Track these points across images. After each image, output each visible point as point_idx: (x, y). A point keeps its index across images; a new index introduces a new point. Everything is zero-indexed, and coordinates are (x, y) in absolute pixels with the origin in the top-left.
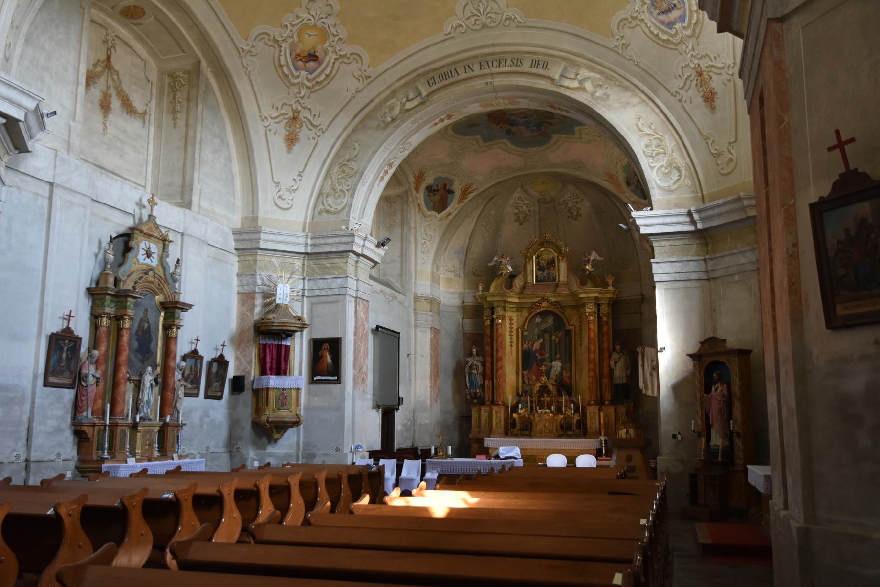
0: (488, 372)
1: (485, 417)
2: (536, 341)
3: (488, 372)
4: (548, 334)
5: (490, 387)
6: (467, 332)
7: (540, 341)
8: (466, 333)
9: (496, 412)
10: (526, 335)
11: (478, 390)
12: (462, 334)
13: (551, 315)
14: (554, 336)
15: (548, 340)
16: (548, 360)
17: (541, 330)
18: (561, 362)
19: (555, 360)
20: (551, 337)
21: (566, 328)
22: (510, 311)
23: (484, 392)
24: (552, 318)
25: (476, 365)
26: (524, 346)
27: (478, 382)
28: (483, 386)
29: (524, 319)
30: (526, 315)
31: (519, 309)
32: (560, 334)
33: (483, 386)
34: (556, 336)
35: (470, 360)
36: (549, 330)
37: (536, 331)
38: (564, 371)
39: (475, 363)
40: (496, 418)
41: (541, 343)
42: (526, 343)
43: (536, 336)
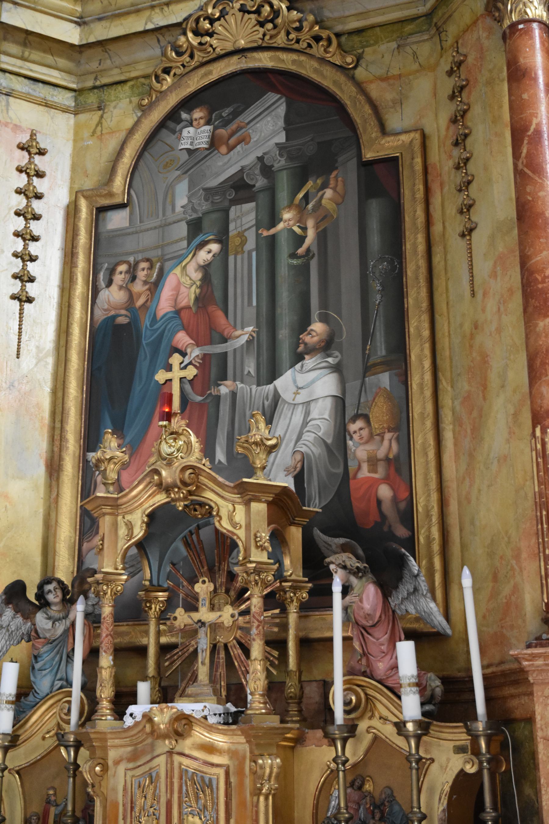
2: (179, 258)
4: (252, 205)
7: (203, 256)
10: (120, 233)
13: (272, 97)
14: (287, 215)
15: (251, 244)
16: (251, 367)
17: (209, 192)
18: (337, 369)
19: (299, 358)
20: (274, 220)
21: (369, 155)
22: (28, 98)
24: (282, 110)
26: (104, 295)
29: (113, 144)
30: (129, 122)
31: (92, 99)
32: (329, 193)
34: (301, 209)
36: (260, 182)
37: (181, 200)
38: (353, 427)
41: (205, 268)
42: (118, 278)
43: (182, 230)
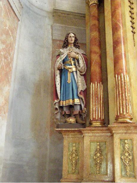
0: (95, 68)
1: (93, 153)
3: (95, 68)
5: (101, 93)
6: (57, 38)
8: (56, 40)
9: (121, 140)
11: (77, 101)
12: (51, 41)
23: (87, 105)
25: (74, 59)
27: (77, 88)
28: (86, 92)
33: (86, 92)
35: (65, 52)
39: (73, 54)
40: (123, 154)
